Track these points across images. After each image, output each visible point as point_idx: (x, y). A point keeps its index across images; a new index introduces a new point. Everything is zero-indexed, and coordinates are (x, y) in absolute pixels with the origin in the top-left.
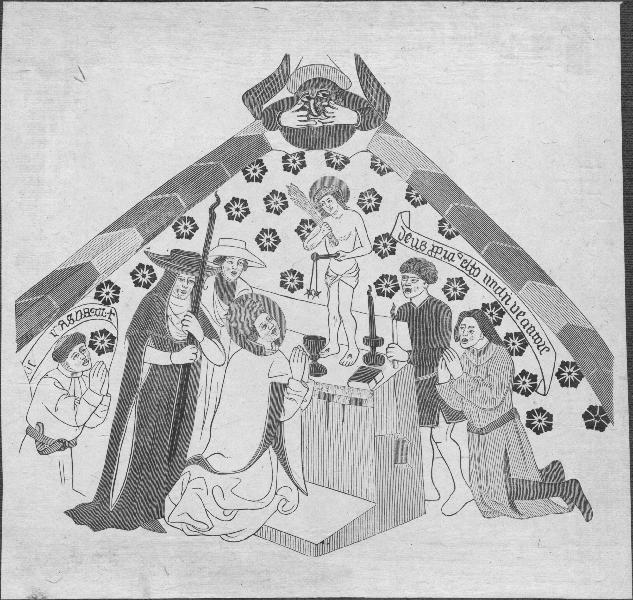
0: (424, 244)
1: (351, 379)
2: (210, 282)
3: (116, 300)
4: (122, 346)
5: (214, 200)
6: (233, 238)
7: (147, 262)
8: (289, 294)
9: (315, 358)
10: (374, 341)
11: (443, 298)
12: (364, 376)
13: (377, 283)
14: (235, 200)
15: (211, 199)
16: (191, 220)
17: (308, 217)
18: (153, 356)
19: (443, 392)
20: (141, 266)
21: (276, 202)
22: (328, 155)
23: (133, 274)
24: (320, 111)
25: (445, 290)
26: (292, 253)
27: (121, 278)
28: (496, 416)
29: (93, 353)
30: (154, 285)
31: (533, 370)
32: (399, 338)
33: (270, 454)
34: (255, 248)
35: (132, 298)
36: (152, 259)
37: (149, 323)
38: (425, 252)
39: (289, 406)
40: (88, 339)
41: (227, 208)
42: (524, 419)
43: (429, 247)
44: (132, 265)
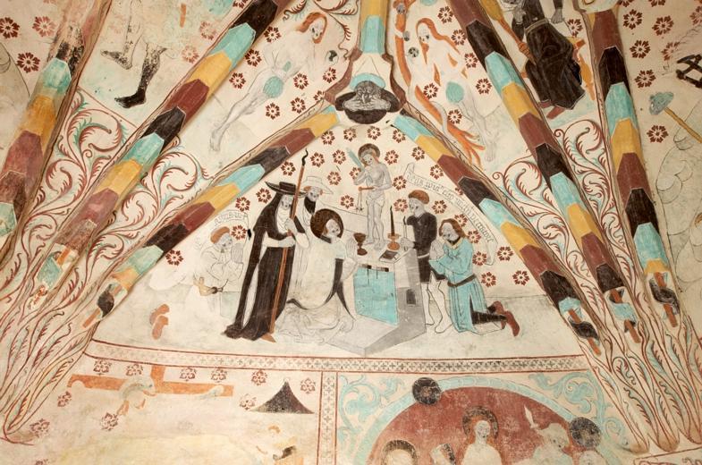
0: (421, 182)
3: (247, 208)
8: (345, 209)
9: (360, 245)
11: (432, 212)
12: (387, 256)
13: (395, 204)
14: (316, 155)
15: (302, 153)
16: (291, 164)
17: (357, 167)
18: (268, 242)
19: (432, 263)
20: (262, 190)
21: (339, 157)
23: (258, 194)
24: (368, 100)
25: (434, 207)
26: (348, 186)
27: (251, 195)
28: (465, 277)
29: (234, 238)
30: (269, 201)
31: (482, 252)
32: (408, 235)
33: (336, 297)
34: (327, 182)
35: (257, 209)
37: (267, 222)
39: (345, 271)
40: (232, 230)
41: (312, 159)
42: (481, 279)
43: (424, 184)
44: (257, 189)
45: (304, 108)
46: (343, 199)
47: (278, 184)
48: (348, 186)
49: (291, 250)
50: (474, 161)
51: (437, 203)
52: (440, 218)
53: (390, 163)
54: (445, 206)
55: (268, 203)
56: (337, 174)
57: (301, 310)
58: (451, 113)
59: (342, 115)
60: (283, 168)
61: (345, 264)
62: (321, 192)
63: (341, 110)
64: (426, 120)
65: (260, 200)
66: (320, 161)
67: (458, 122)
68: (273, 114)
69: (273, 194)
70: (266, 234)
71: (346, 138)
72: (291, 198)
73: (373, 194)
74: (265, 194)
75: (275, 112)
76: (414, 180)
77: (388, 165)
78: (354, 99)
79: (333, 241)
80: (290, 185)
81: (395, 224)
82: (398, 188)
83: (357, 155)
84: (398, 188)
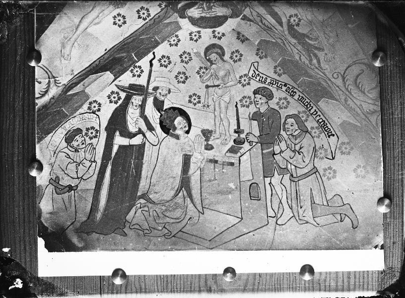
1: (227, 152)
2: (150, 101)
4: (103, 135)
5: (153, 56)
6: (161, 79)
7: (116, 90)
8: (193, 107)
9: (207, 140)
10: (238, 131)
11: (277, 108)
13: (241, 101)
15: (150, 56)
16: (140, 67)
17: (203, 66)
18: (120, 141)
21: (185, 57)
22: (214, 32)
23: (109, 97)
27: (102, 98)
30: (120, 102)
36: (118, 88)
37: (117, 123)
38: (267, 83)
39: (193, 167)
41: (160, 60)
43: (269, 80)
44: (108, 91)
45: (149, 15)
46: (190, 97)
47: (127, 85)
48: (196, 85)
49: (142, 147)
50: (315, 61)
51: (280, 99)
52: (284, 113)
53: (235, 61)
54: (288, 102)
55: (118, 105)
56: (184, 73)
57: (150, 205)
58: (291, 16)
59: (185, 23)
60: (132, 71)
61: (193, 160)
62: (169, 92)
63: (185, 18)
64: (266, 23)
65: (111, 102)
66: (167, 62)
67: (298, 25)
68: (120, 23)
69: (123, 95)
70: (117, 133)
71: (191, 39)
72: (141, 98)
73: (220, 92)
74: (116, 95)
75: (122, 21)
76: (258, 78)
77: (232, 63)
78: (195, 7)
79: (182, 138)
80: (140, 86)
81: (240, 119)
82: (244, 86)
83: (203, 54)
84: (244, 86)
